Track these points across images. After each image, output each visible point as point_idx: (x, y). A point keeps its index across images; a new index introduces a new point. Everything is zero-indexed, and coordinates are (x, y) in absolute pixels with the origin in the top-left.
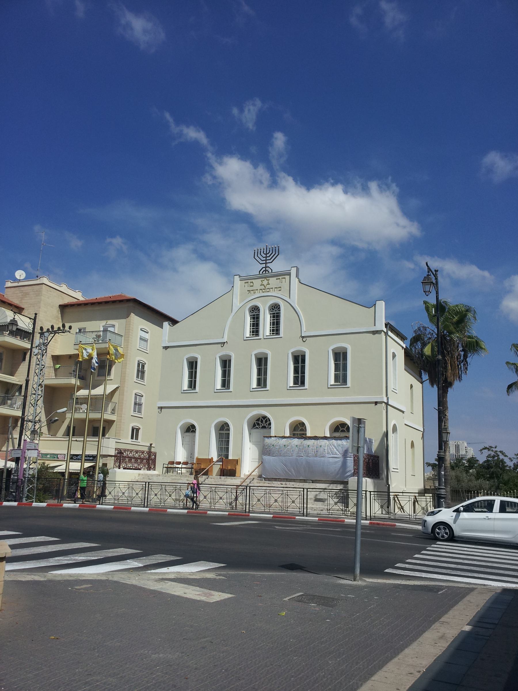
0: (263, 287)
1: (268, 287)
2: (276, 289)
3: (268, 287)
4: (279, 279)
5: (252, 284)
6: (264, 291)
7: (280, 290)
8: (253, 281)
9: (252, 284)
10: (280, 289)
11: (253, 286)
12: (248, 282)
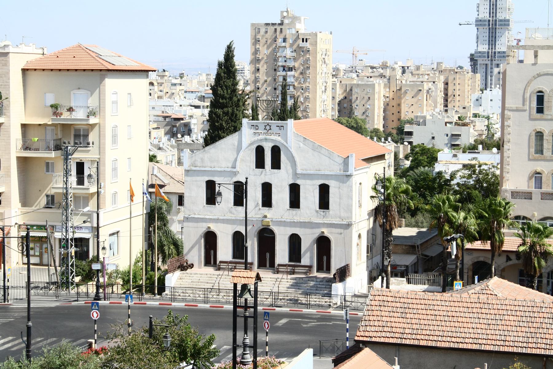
0: (265, 131)
5: (257, 128)
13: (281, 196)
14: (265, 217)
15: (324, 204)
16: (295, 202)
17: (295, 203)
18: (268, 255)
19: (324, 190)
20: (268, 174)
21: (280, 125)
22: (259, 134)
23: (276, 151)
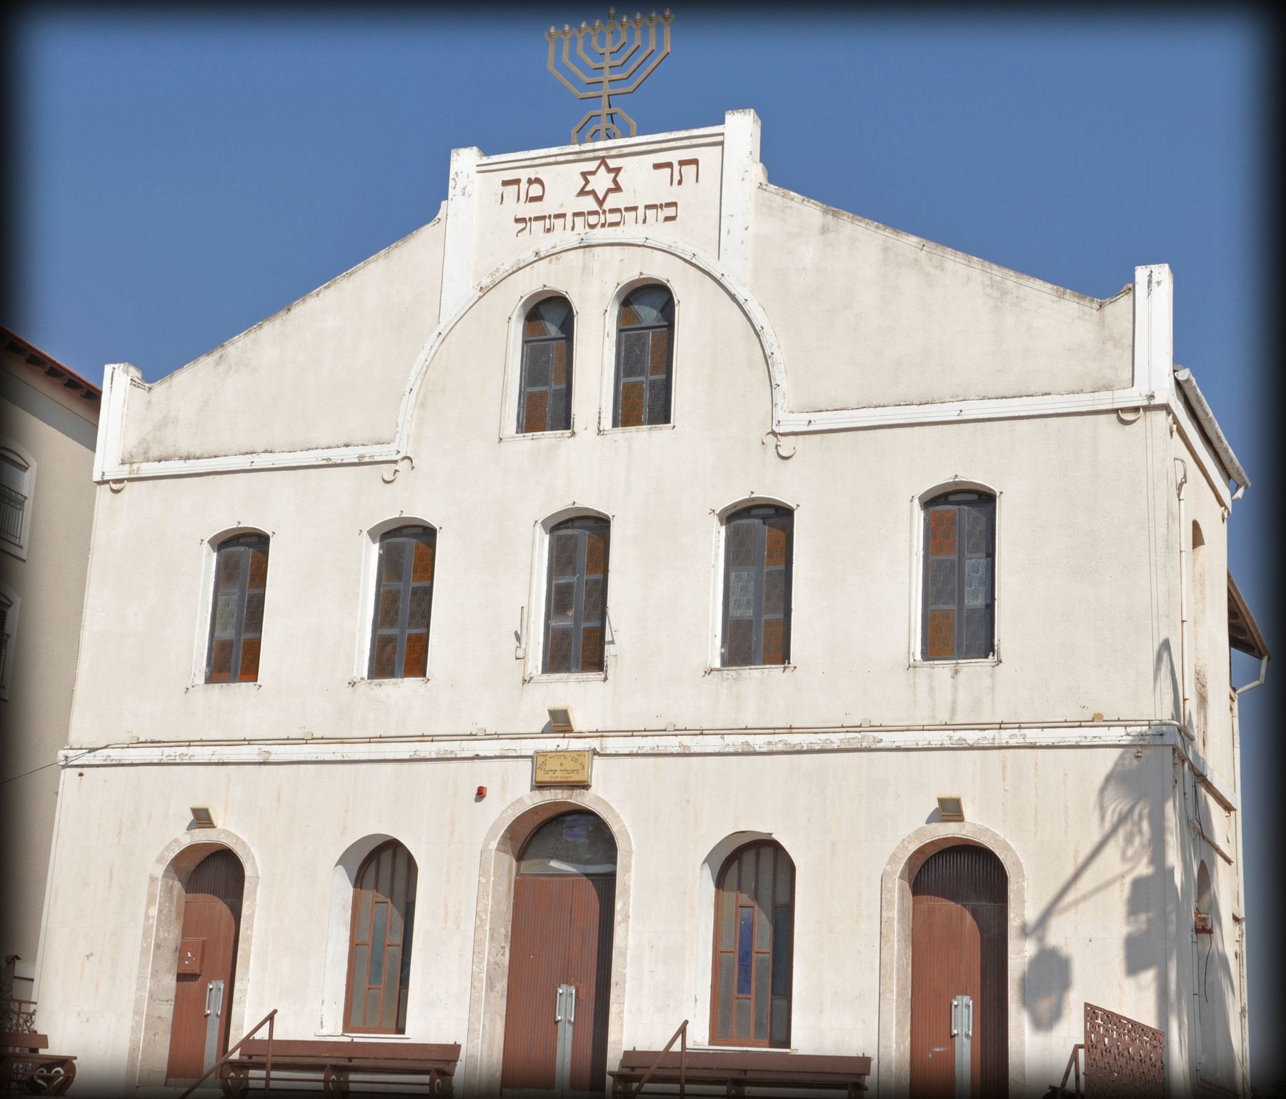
0: (589, 204)
1: (613, 201)
2: (651, 213)
3: (613, 201)
4: (670, 165)
5: (535, 190)
6: (593, 220)
7: (667, 219)
8: (541, 173)
9: (535, 190)
10: (670, 212)
11: (539, 199)
12: (517, 182)
13: (668, 591)
14: (560, 722)
15: (959, 620)
16: (758, 630)
17: (758, 630)
18: (566, 996)
19: (961, 520)
20: (594, 462)
21: (673, 157)
22: (548, 221)
23: (648, 308)
